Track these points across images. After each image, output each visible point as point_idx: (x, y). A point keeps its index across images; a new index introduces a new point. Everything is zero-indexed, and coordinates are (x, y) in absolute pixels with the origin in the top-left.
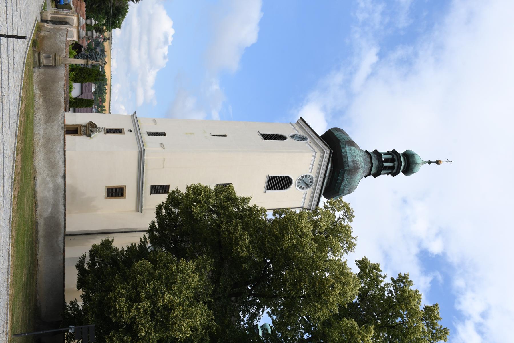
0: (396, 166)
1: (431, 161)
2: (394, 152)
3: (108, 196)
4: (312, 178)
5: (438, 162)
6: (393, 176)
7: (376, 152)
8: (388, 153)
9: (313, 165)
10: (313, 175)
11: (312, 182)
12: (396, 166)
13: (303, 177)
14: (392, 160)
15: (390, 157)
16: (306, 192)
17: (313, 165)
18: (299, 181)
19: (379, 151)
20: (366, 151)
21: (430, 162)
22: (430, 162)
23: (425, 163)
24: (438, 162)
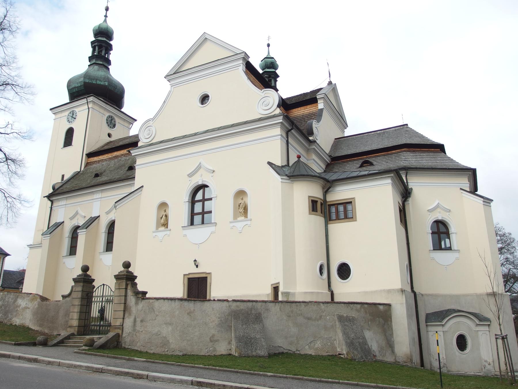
0: (106, 45)
1: (105, 15)
2: (92, 43)
3: (189, 279)
4: (109, 116)
5: (107, 9)
6: (112, 50)
7: (90, 59)
8: (94, 48)
9: (100, 112)
10: (107, 114)
11: (112, 117)
12: (106, 45)
13: (107, 123)
14: (100, 47)
15: (97, 48)
16: (119, 123)
17: (100, 112)
18: (109, 126)
19: (90, 55)
20: (89, 66)
21: (106, 16)
22: (106, 16)
23: (105, 21)
24: (107, 9)
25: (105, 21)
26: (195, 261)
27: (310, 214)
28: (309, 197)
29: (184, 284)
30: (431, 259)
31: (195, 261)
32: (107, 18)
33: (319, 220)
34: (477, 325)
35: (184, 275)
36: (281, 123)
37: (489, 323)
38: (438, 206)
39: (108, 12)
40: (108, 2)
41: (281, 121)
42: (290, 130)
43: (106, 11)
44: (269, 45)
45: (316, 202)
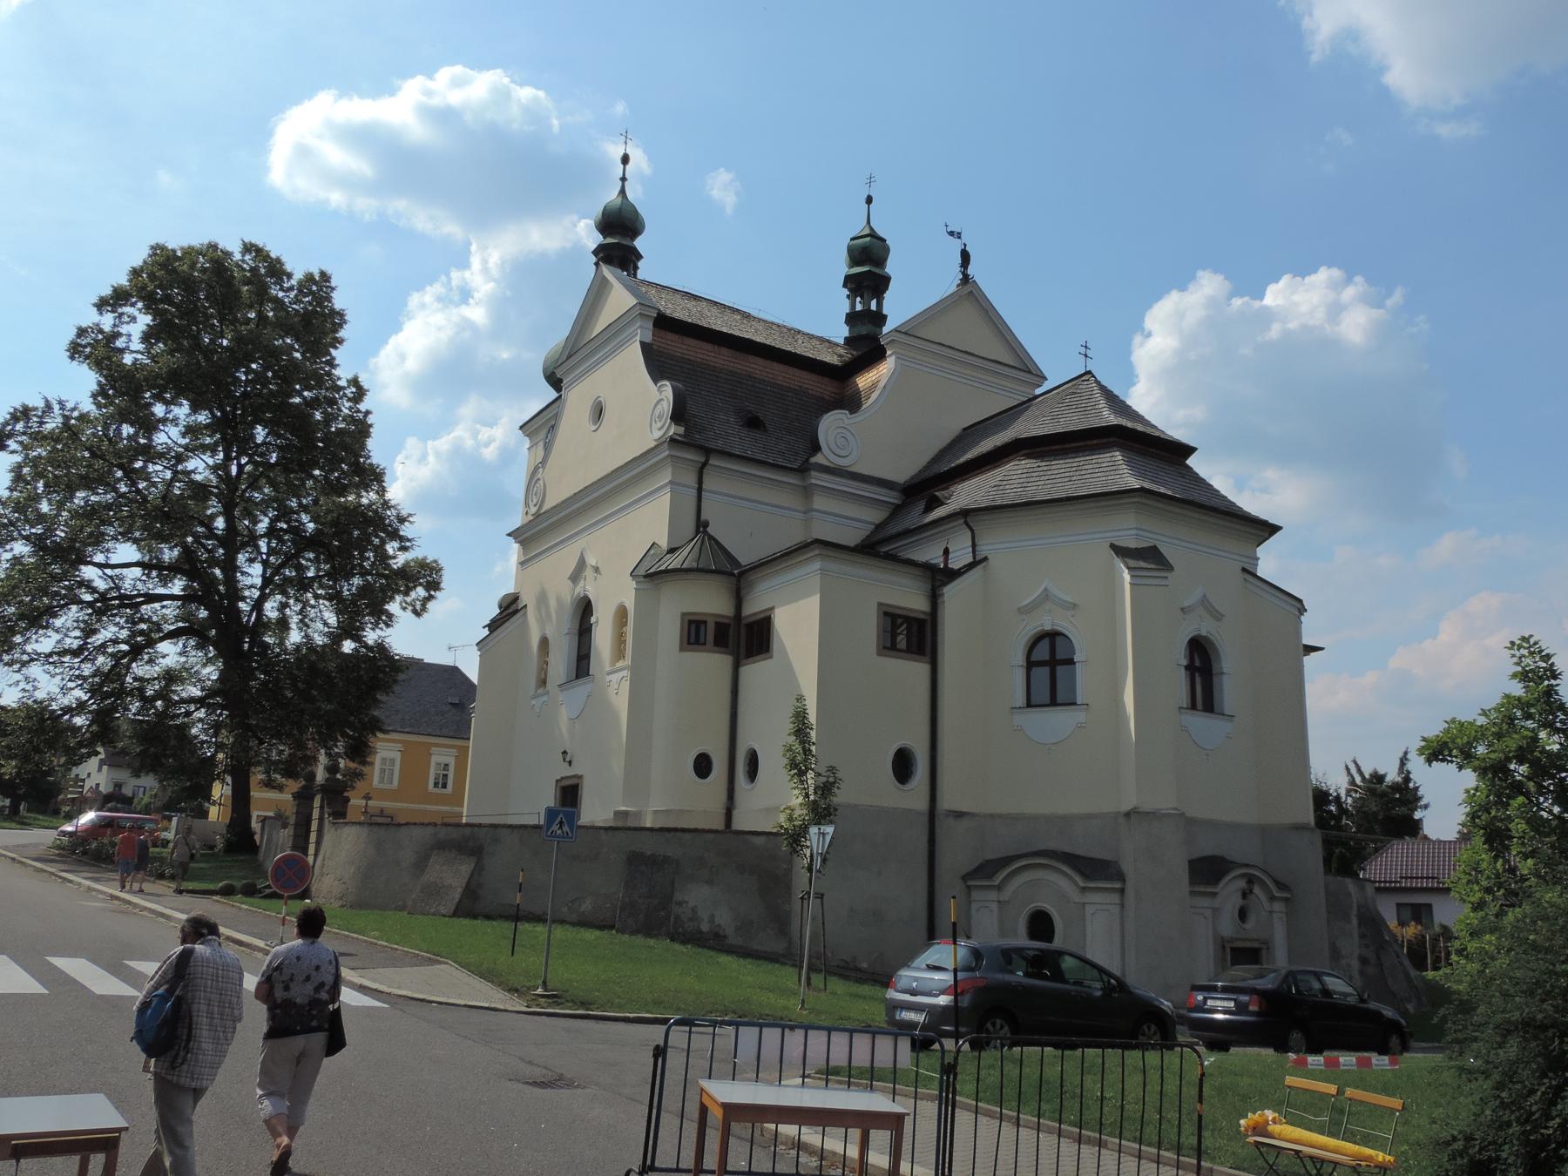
1: (621, 175)
21: (623, 179)
23: (623, 192)
25: (623, 192)
26: (565, 753)
27: (682, 649)
28: (683, 615)
29: (555, 799)
30: (1015, 730)
31: (565, 753)
32: (626, 183)
33: (715, 664)
34: (1084, 889)
35: (557, 781)
36: (669, 455)
37: (1118, 885)
38: (1046, 596)
39: (627, 167)
40: (628, 141)
41: (667, 453)
42: (704, 465)
43: (622, 166)
44: (869, 200)
45: (705, 622)
